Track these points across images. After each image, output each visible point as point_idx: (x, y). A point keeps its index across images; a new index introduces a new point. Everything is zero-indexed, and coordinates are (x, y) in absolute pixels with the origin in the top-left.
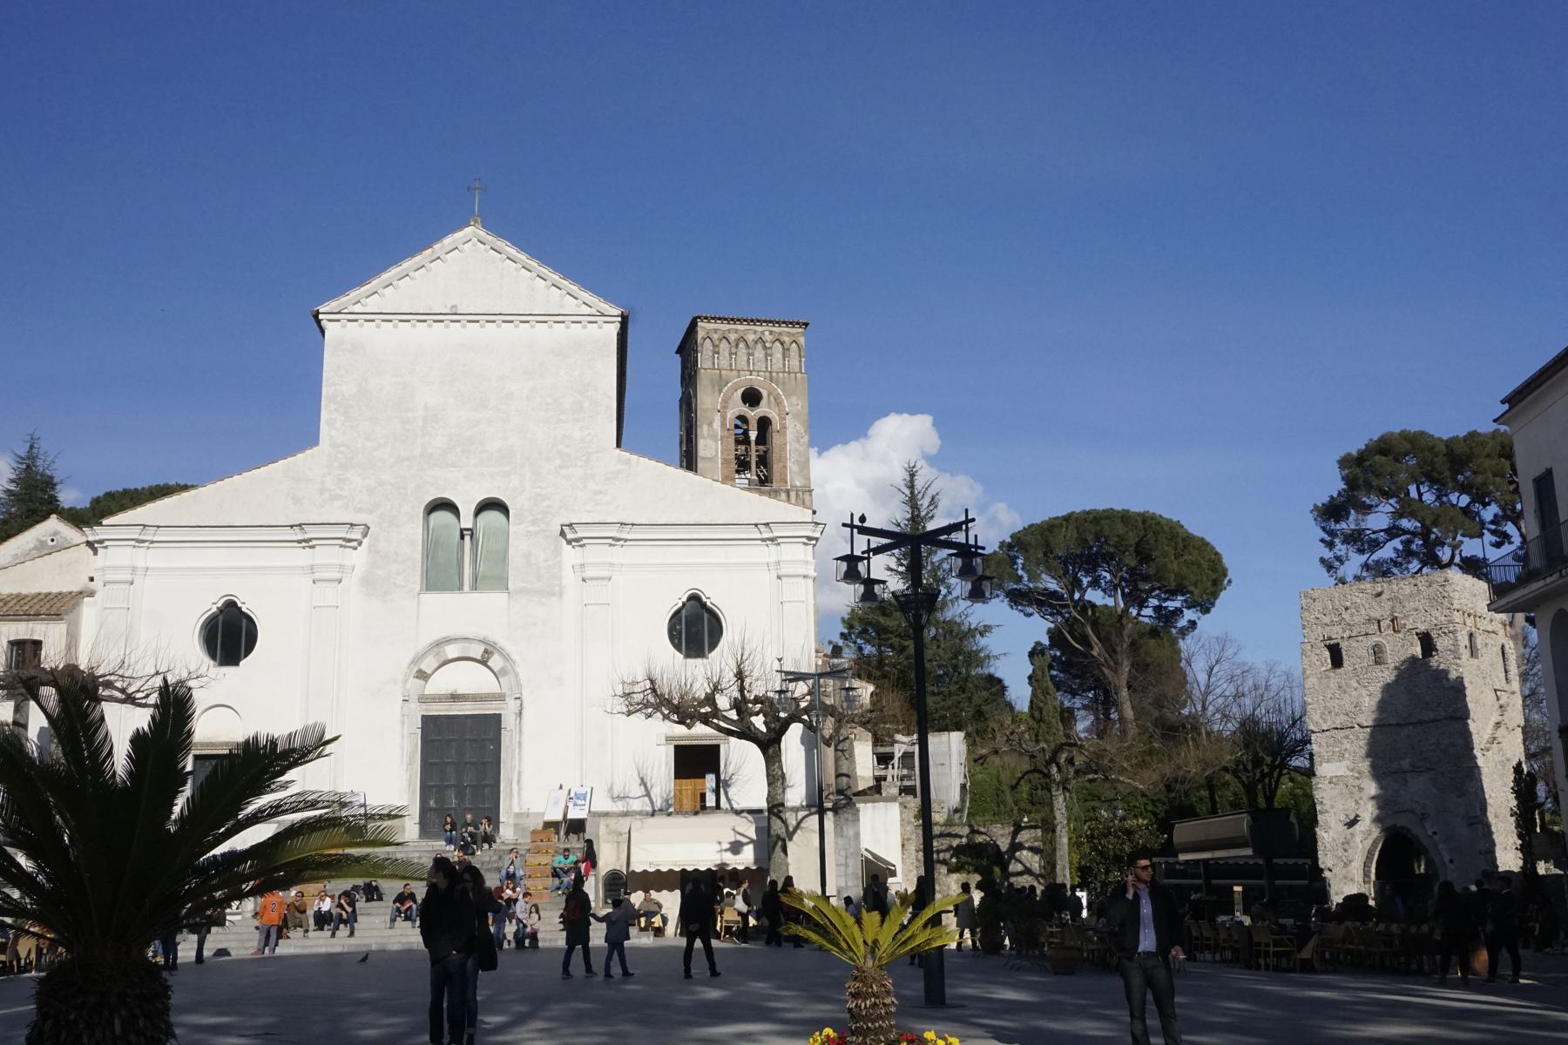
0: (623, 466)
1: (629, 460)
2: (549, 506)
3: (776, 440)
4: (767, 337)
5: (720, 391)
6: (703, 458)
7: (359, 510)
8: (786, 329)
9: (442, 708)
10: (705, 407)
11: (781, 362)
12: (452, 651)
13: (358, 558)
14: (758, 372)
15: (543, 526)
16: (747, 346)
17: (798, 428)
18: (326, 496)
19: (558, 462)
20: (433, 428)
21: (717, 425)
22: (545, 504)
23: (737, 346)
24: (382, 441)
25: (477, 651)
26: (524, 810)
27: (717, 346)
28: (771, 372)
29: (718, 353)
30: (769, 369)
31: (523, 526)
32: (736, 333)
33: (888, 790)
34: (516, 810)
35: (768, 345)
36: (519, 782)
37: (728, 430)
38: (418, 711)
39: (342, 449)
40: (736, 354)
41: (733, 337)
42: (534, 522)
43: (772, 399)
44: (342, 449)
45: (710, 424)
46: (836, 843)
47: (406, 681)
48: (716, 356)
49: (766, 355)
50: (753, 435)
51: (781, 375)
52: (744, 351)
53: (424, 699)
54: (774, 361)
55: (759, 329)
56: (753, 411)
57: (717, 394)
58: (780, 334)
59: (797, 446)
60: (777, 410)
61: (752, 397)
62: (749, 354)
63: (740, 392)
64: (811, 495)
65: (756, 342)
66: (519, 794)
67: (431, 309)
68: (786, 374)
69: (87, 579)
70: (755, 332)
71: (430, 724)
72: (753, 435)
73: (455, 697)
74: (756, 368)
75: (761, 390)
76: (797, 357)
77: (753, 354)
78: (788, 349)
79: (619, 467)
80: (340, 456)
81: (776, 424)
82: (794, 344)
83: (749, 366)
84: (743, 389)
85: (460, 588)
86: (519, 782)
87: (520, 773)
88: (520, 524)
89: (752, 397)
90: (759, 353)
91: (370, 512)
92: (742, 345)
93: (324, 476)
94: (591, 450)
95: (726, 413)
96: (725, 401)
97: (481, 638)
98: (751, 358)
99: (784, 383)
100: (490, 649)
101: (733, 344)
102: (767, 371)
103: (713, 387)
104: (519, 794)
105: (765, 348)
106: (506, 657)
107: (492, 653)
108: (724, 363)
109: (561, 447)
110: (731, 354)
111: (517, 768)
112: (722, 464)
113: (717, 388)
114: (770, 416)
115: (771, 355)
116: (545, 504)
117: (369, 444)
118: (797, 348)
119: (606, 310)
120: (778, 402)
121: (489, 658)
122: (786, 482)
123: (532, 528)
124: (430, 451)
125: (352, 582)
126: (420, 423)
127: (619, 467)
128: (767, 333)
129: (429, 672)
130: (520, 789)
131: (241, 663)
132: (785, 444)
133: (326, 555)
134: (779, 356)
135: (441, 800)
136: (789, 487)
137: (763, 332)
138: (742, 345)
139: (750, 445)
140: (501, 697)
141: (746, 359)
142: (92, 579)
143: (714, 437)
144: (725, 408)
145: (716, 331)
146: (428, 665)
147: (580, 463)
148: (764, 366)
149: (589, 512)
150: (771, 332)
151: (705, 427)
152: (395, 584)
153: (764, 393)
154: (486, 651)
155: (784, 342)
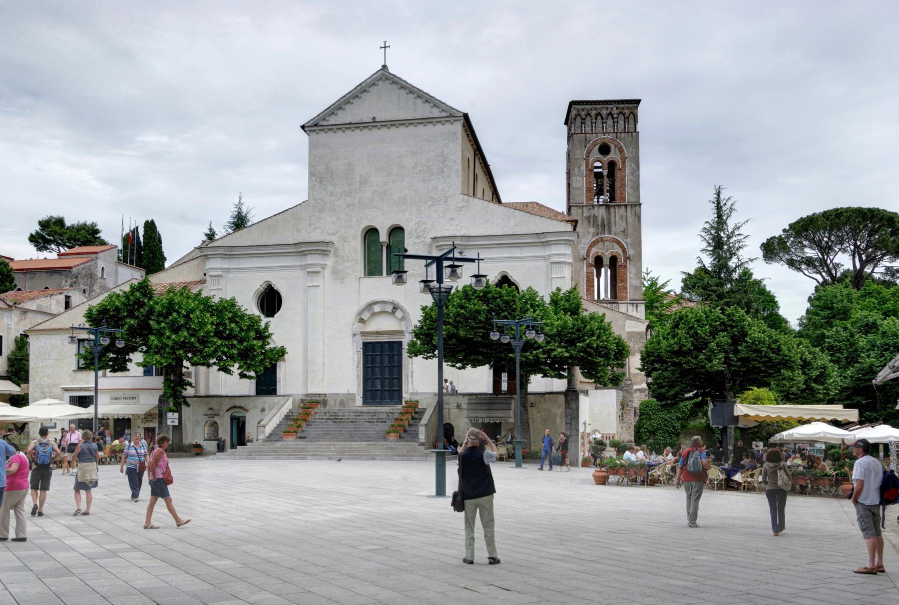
0: (465, 204)
1: (468, 200)
2: (425, 228)
3: (618, 175)
4: (615, 111)
5: (585, 147)
6: (575, 188)
7: (329, 234)
8: (627, 105)
9: (373, 338)
10: (576, 157)
11: (623, 126)
12: (377, 309)
13: (329, 261)
14: (609, 133)
15: (423, 239)
16: (602, 118)
18: (313, 227)
19: (430, 203)
20: (365, 187)
21: (583, 167)
22: (423, 226)
23: (596, 119)
24: (339, 196)
25: (389, 308)
26: (415, 391)
27: (585, 119)
28: (616, 133)
29: (584, 123)
30: (616, 131)
31: (412, 239)
32: (596, 110)
33: (626, 382)
34: (411, 391)
35: (615, 116)
36: (412, 377)
38: (360, 340)
39: (319, 201)
40: (595, 123)
41: (593, 113)
42: (418, 237)
43: (617, 150)
44: (319, 201)
45: (579, 167)
46: (566, 412)
47: (353, 324)
48: (583, 125)
49: (614, 123)
51: (623, 134)
52: (600, 121)
53: (363, 334)
54: (619, 126)
56: (605, 157)
57: (583, 149)
58: (623, 108)
59: (632, 177)
60: (620, 156)
61: (604, 149)
62: (603, 123)
63: (597, 147)
64: (640, 207)
65: (608, 115)
66: (412, 383)
67: (362, 120)
68: (626, 134)
69: (203, 275)
70: (607, 108)
71: (366, 345)
73: (378, 333)
74: (608, 131)
75: (610, 144)
76: (633, 122)
77: (606, 123)
78: (628, 118)
79: (463, 204)
80: (318, 205)
81: (619, 165)
82: (632, 115)
83: (603, 130)
84: (599, 145)
85: (381, 274)
86: (412, 377)
87: (412, 372)
88: (410, 238)
89: (604, 149)
90: (610, 122)
91: (334, 235)
92: (599, 117)
93: (311, 217)
94: (448, 195)
95: (589, 160)
96: (589, 153)
97: (391, 301)
98: (605, 125)
99: (624, 139)
100: (396, 306)
101: (594, 117)
102: (614, 132)
103: (581, 143)
104: (412, 383)
105: (613, 118)
106: (403, 311)
107: (397, 309)
108: (588, 129)
109: (431, 194)
110: (592, 123)
111: (411, 370)
112: (586, 191)
113: (583, 145)
114: (616, 160)
115: (617, 122)
116: (423, 226)
117: (333, 198)
118: (633, 117)
119: (455, 113)
120: (621, 151)
121: (395, 312)
122: (625, 200)
123: (417, 241)
124: (363, 200)
125: (327, 272)
126: (358, 185)
127: (463, 204)
128: (615, 109)
129: (365, 319)
130: (412, 380)
131: (275, 316)
132: (625, 177)
133: (310, 260)
134: (622, 122)
135: (373, 385)
136: (627, 203)
137: (612, 109)
138: (599, 117)
139: (603, 178)
140: (401, 333)
141: (601, 126)
142: (205, 275)
143: (581, 175)
144: (589, 157)
145: (583, 110)
146: (366, 316)
147: (442, 203)
148: (590, 129)
149: (447, 230)
151: (576, 169)
152: (347, 273)
153: (612, 146)
154: (394, 308)
155: (625, 113)
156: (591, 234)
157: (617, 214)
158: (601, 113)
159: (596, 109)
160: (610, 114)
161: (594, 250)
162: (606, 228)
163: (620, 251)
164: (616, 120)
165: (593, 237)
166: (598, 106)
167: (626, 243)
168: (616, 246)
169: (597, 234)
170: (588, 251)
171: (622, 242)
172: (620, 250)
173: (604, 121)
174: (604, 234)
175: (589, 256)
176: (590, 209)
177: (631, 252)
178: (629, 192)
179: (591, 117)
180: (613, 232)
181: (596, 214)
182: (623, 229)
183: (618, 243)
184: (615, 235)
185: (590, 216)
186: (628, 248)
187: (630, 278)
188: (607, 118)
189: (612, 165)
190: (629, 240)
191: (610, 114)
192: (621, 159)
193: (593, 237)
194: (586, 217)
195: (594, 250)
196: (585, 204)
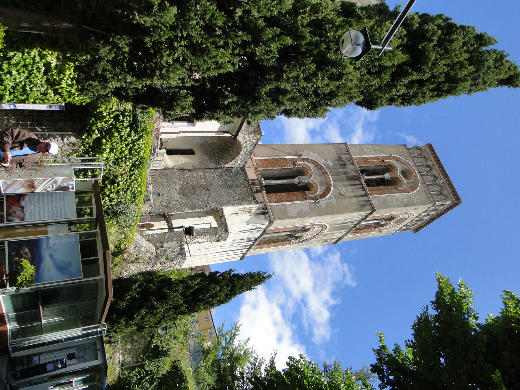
8: (450, 191)
11: (432, 190)
17: (404, 200)
37: (383, 161)
41: (430, 163)
48: (416, 155)
50: (387, 176)
54: (430, 186)
55: (442, 177)
58: (446, 188)
72: (387, 176)
105: (434, 180)
132: (392, 193)
134: (435, 190)
137: (441, 179)
138: (428, 169)
145: (428, 154)
150: (443, 183)
155: (444, 191)
156: (326, 163)
157: (355, 187)
158: (433, 170)
159: (434, 165)
160: (436, 178)
161: (311, 166)
162: (338, 177)
163: (319, 192)
164: (434, 183)
165: (323, 164)
166: (437, 166)
167: (330, 198)
168: (324, 188)
169: (328, 168)
170: (308, 160)
171: (330, 193)
172: (321, 193)
173: (428, 172)
174: (331, 175)
175: (304, 161)
176: (349, 161)
177: (323, 202)
178: (381, 199)
179: (426, 161)
180: (336, 183)
181: (347, 167)
182: (343, 193)
183: (328, 190)
184: (335, 186)
185: (344, 161)
186: (326, 200)
187: (295, 205)
188: (431, 176)
189: (393, 183)
190: (334, 200)
191: (436, 178)
192: (405, 188)
193: (326, 165)
194: (340, 157)
195: (311, 166)
196: (353, 157)
